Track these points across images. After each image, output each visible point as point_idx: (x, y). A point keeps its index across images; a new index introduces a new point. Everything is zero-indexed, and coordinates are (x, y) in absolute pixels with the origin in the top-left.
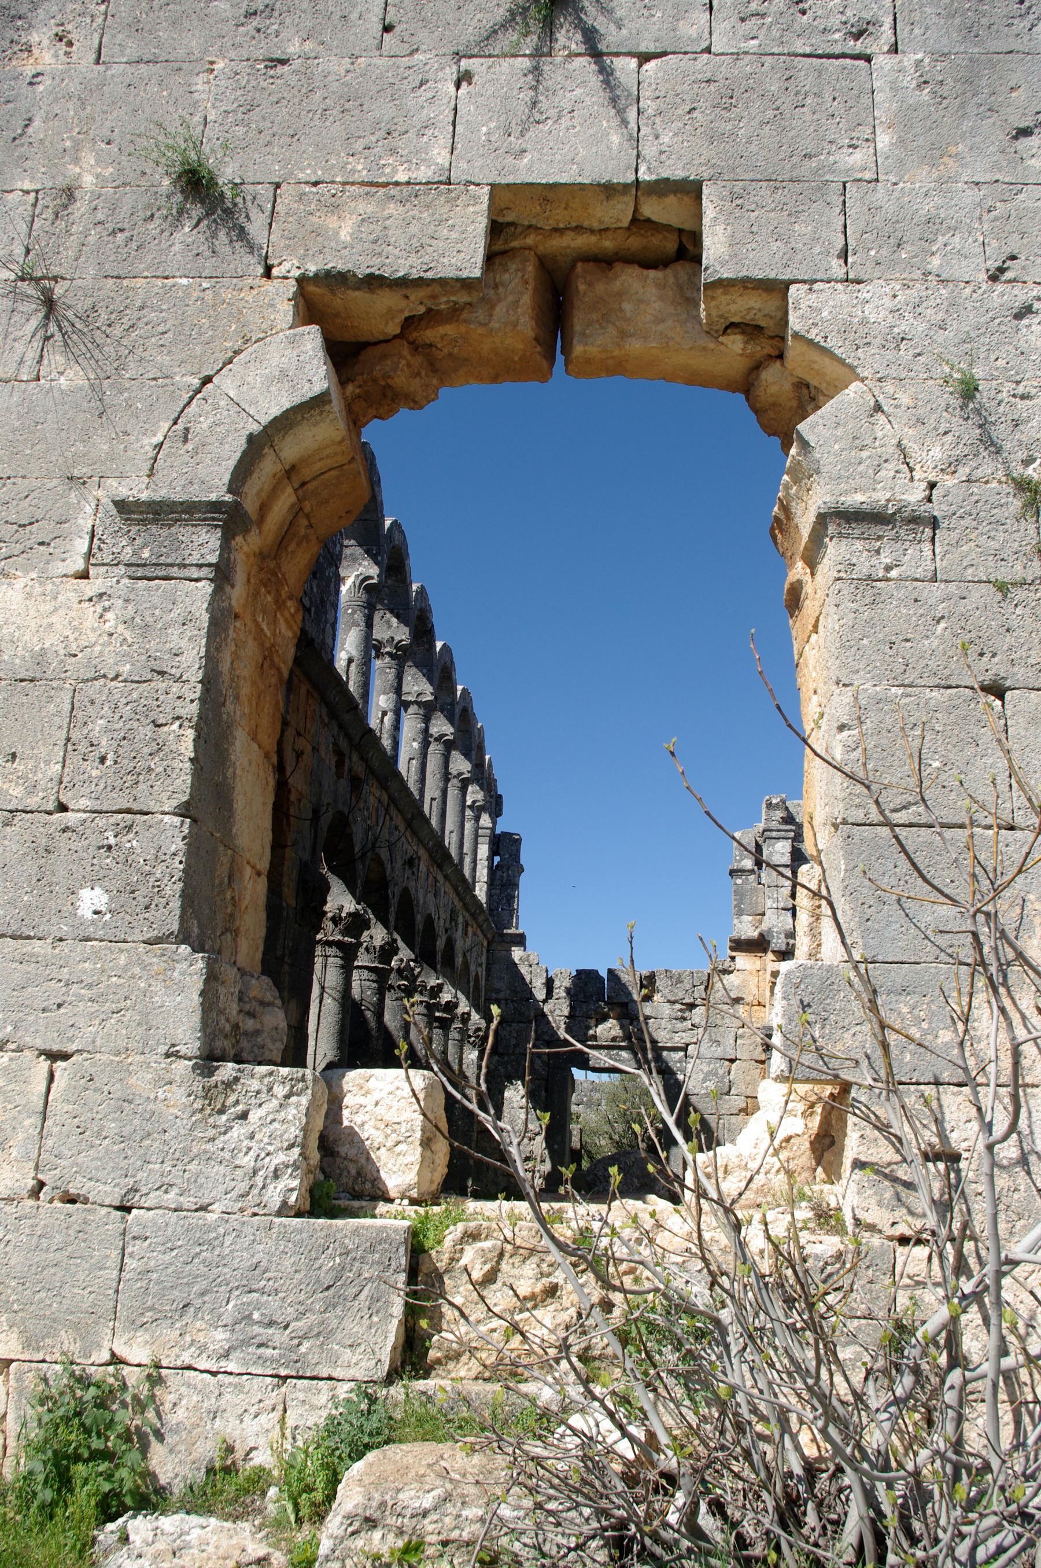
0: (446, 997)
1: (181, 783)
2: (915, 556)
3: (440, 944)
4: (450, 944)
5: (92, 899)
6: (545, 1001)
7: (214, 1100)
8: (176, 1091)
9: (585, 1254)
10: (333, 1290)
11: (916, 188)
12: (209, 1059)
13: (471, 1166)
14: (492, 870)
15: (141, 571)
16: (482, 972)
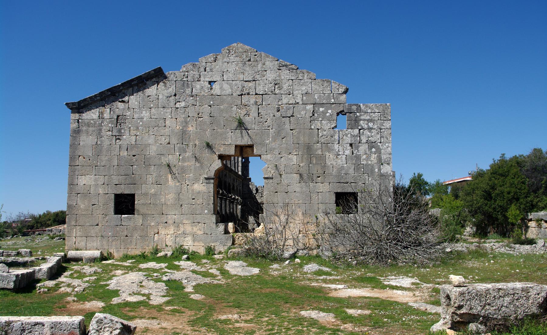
0: (233, 197)
1: (212, 202)
2: (271, 181)
3: (231, 187)
4: (233, 186)
5: (206, 211)
6: (256, 194)
7: (217, 226)
8: (214, 226)
9: (246, 236)
10: (227, 239)
11: (273, 145)
12: (216, 223)
13: (236, 231)
14: (242, 163)
15: (207, 183)
16: (241, 188)
